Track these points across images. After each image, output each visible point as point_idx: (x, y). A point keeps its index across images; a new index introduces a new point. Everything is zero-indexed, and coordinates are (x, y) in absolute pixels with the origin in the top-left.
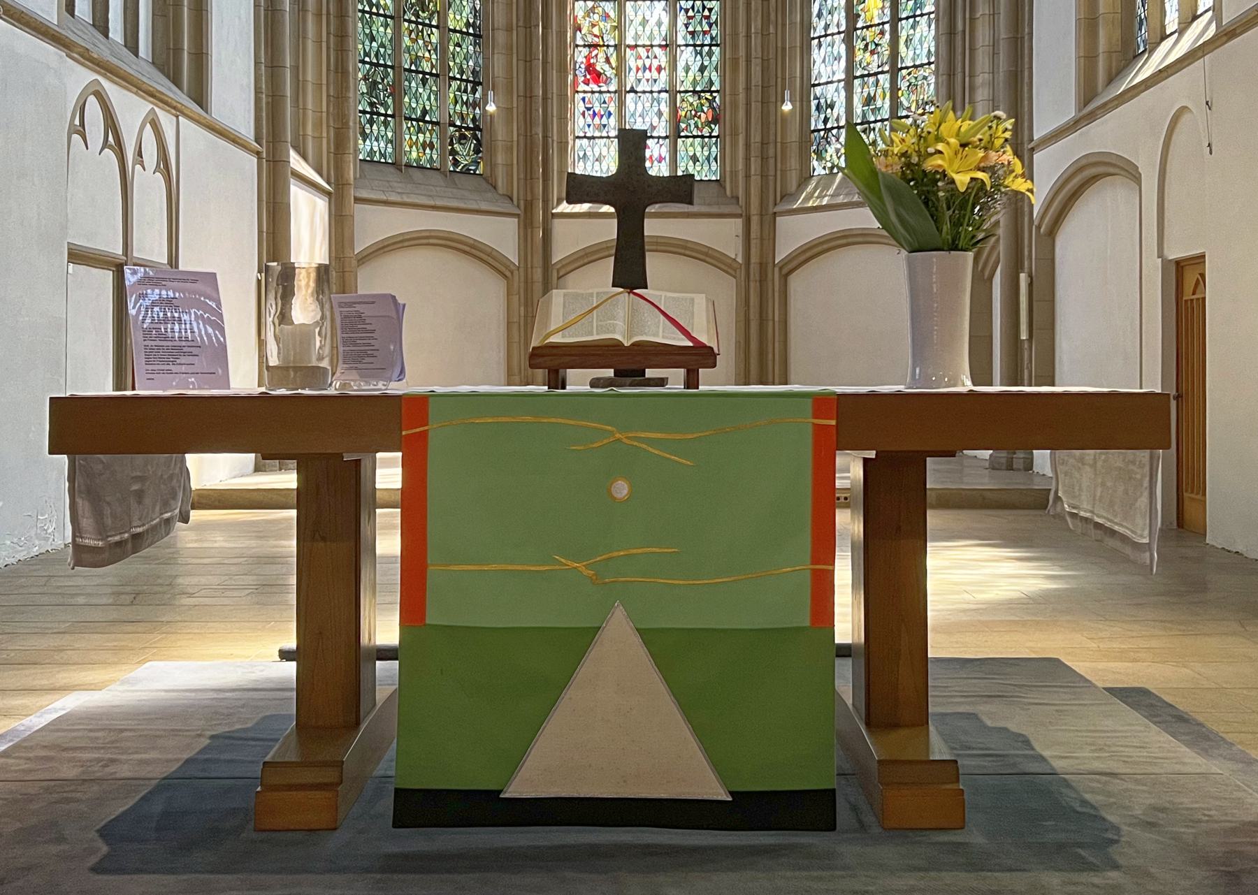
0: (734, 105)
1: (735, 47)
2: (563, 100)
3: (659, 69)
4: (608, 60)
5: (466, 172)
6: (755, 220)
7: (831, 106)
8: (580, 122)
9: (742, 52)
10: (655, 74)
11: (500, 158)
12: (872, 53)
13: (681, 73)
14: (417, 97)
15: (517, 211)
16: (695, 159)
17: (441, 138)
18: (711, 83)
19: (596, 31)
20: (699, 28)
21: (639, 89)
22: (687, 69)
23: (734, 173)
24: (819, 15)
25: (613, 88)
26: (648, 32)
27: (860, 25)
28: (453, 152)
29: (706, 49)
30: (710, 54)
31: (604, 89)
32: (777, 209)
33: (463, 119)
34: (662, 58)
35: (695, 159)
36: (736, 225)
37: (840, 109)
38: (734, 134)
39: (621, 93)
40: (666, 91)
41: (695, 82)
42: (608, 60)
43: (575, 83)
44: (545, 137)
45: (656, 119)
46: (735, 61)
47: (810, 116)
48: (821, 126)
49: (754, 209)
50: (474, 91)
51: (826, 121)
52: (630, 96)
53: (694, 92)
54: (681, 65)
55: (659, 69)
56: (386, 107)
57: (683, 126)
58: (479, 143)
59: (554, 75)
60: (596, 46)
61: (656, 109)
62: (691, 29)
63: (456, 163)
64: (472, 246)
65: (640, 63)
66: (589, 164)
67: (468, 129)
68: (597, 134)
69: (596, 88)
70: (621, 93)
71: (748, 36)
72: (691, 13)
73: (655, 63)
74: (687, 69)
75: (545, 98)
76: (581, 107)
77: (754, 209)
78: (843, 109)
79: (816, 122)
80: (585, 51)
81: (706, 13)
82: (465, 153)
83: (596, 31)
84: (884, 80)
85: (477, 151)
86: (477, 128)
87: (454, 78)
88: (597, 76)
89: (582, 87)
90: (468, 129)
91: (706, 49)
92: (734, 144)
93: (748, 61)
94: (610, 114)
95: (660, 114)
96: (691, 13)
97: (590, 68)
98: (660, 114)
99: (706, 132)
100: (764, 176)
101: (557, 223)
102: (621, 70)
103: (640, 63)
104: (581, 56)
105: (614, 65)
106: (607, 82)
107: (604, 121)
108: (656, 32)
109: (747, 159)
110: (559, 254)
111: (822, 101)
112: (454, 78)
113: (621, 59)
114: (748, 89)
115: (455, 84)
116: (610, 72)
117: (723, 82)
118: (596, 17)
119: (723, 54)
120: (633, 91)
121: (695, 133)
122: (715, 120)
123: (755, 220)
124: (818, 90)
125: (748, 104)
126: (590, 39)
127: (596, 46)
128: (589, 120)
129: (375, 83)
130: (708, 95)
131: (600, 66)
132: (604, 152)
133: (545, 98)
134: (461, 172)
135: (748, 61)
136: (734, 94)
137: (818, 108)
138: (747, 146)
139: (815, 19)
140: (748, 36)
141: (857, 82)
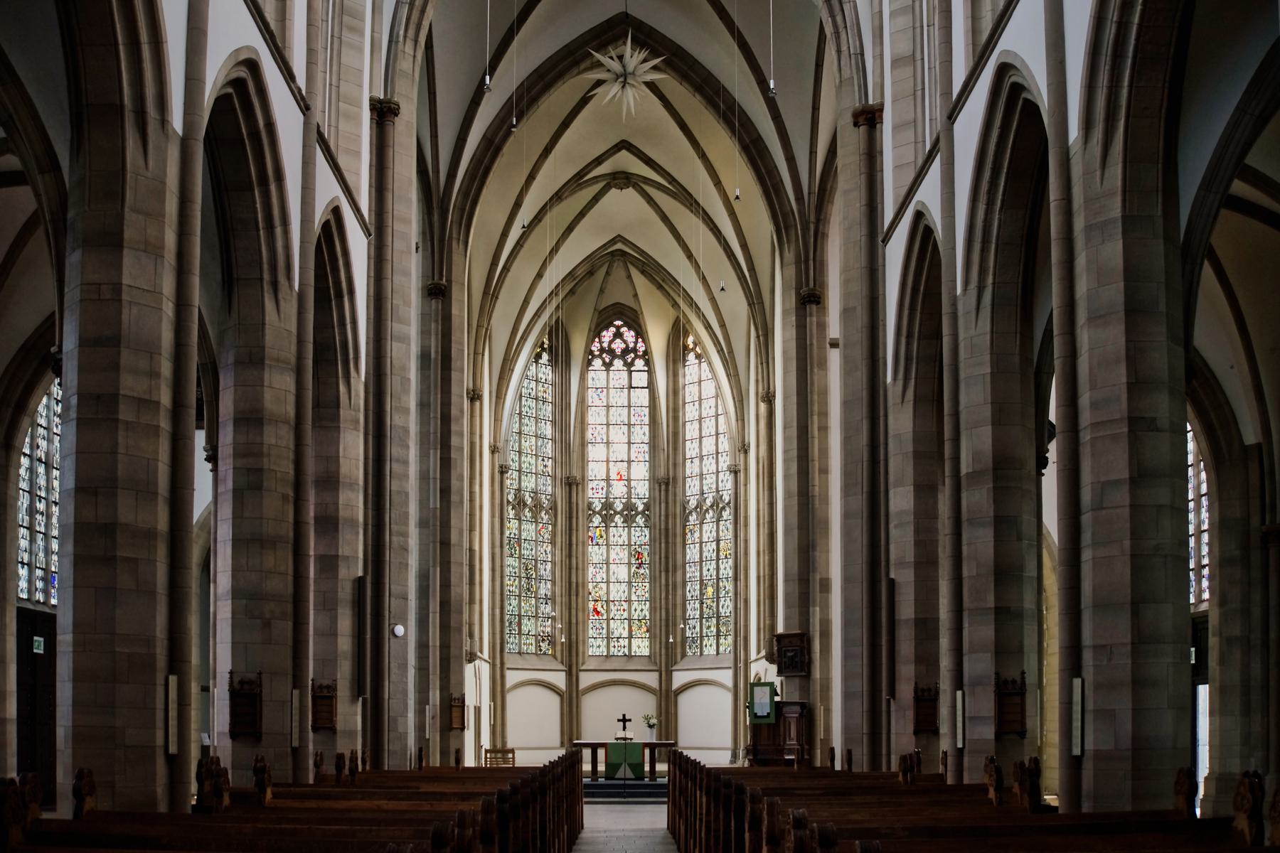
0: (655, 626)
1: (655, 602)
2: (584, 622)
3: (624, 610)
4: (602, 607)
5: (545, 654)
6: (663, 673)
7: (694, 628)
8: (591, 632)
9: (658, 605)
10: (622, 612)
11: (558, 648)
12: (710, 609)
13: (633, 612)
14: (526, 625)
15: (565, 669)
16: (639, 647)
17: (536, 641)
18: (646, 616)
19: (597, 595)
20: (640, 594)
21: (616, 618)
22: (636, 610)
23: (655, 653)
24: (689, 591)
25: (605, 617)
26: (619, 595)
27: (705, 597)
28: (540, 646)
29: (643, 602)
30: (645, 604)
31: (601, 618)
32: (673, 668)
33: (543, 632)
34: (625, 605)
35: (639, 647)
36: (656, 675)
37: (698, 629)
38: (655, 637)
39: (608, 620)
40: (626, 619)
41: (639, 616)
42: (602, 607)
43: (589, 615)
44: (577, 639)
45: (623, 630)
46: (655, 608)
47: (686, 632)
48: (690, 636)
49: (663, 669)
50: (548, 621)
51: (692, 634)
52: (612, 621)
53: (639, 620)
54: (633, 609)
55: (624, 610)
56: (515, 630)
57: (634, 633)
58: (550, 642)
59: (580, 614)
60: (597, 601)
61: (622, 626)
62: (637, 594)
63: (541, 650)
64: (548, 684)
65: (616, 608)
66: (595, 648)
67: (545, 636)
68: (598, 636)
69: (597, 618)
70: (608, 620)
71: (660, 599)
72: (637, 588)
73: (622, 608)
74: (636, 610)
75: (577, 624)
76: (591, 625)
77: (663, 669)
78: (699, 630)
79: (688, 634)
80: (593, 603)
81: (643, 588)
82: (544, 646)
83: (597, 595)
84: (714, 620)
85: (549, 645)
86: (549, 636)
87: (540, 617)
88: (598, 613)
89: (591, 617)
90: (545, 636)
91: (643, 602)
92: (655, 642)
93: (661, 609)
94: (603, 629)
95: (624, 628)
96: (637, 588)
97: (595, 610)
98: (624, 628)
99: (643, 636)
100: (667, 655)
101: (582, 675)
102: (608, 611)
103: (616, 608)
104: (591, 605)
105: (605, 608)
106: (602, 615)
107: (601, 631)
108: (623, 596)
109: (660, 648)
110: (582, 685)
111: (691, 626)
112: (540, 617)
113: (608, 606)
114: (661, 620)
115: (540, 619)
116: (603, 612)
117: (650, 615)
118: (597, 589)
119: (651, 604)
120: (613, 619)
121: (639, 636)
122: (647, 631)
123: (663, 673)
124: (689, 621)
125: (661, 627)
126: (595, 598)
127: (597, 601)
128: (594, 630)
129: (511, 622)
130: (644, 621)
131: (599, 609)
132: (601, 643)
133: (577, 624)
134: (543, 654)
135: (661, 609)
136: (655, 621)
137: (689, 628)
138: (660, 643)
139: (688, 593)
140: (660, 599)
141: (704, 620)
